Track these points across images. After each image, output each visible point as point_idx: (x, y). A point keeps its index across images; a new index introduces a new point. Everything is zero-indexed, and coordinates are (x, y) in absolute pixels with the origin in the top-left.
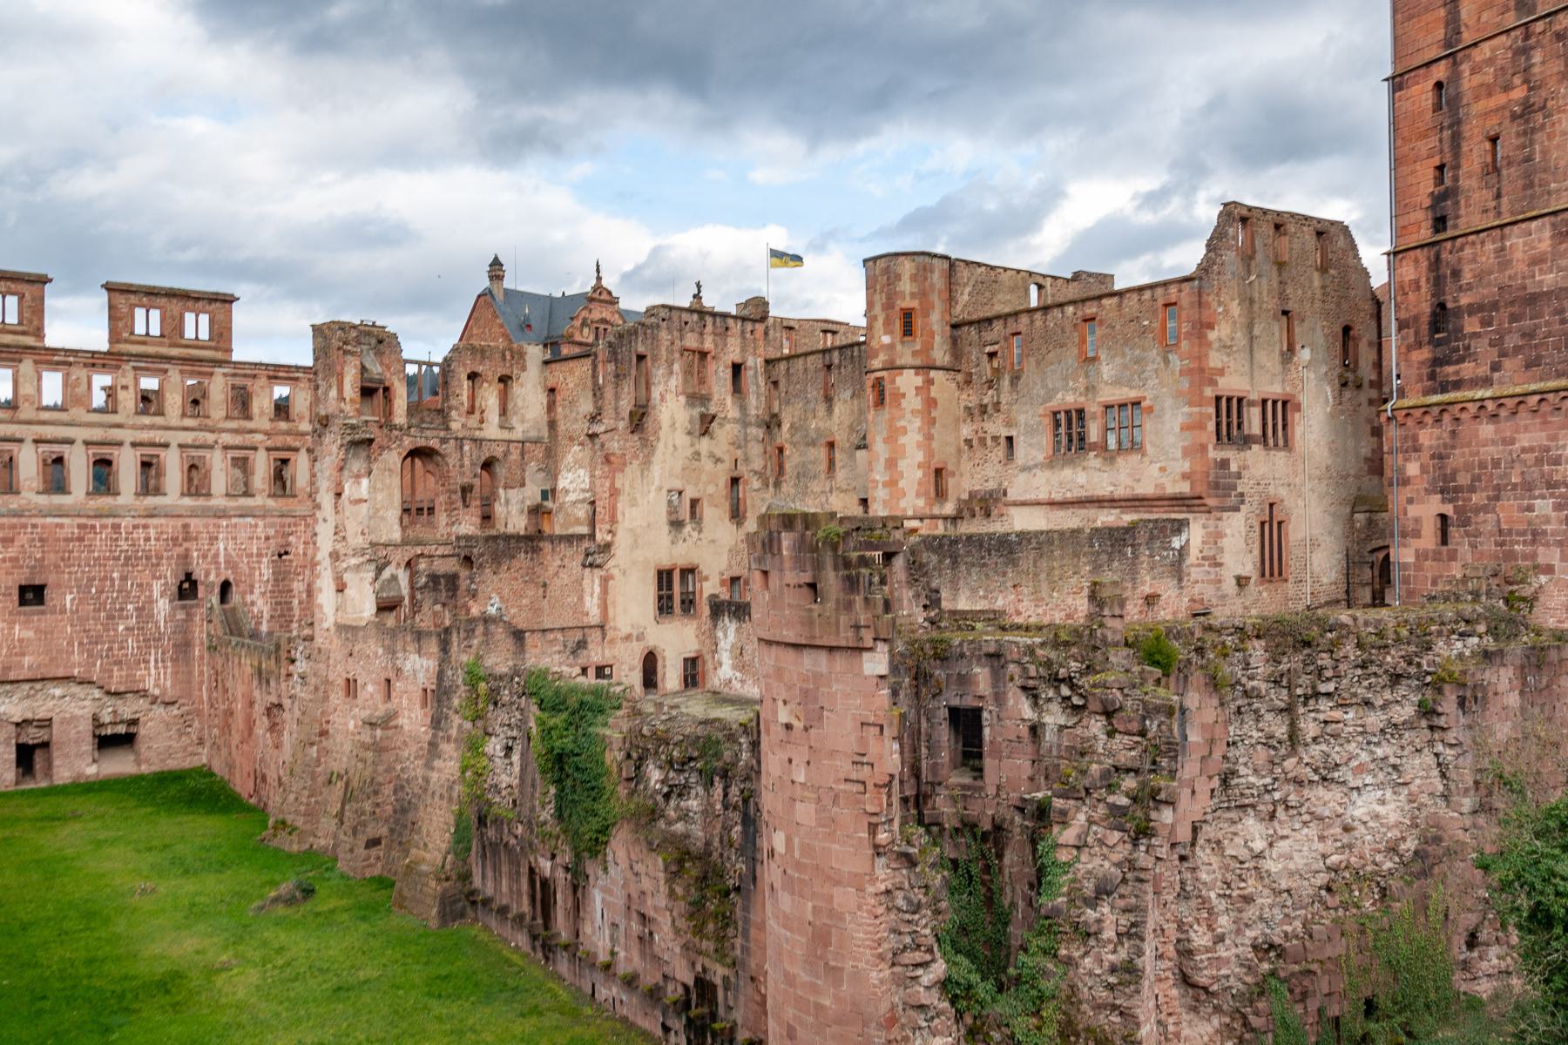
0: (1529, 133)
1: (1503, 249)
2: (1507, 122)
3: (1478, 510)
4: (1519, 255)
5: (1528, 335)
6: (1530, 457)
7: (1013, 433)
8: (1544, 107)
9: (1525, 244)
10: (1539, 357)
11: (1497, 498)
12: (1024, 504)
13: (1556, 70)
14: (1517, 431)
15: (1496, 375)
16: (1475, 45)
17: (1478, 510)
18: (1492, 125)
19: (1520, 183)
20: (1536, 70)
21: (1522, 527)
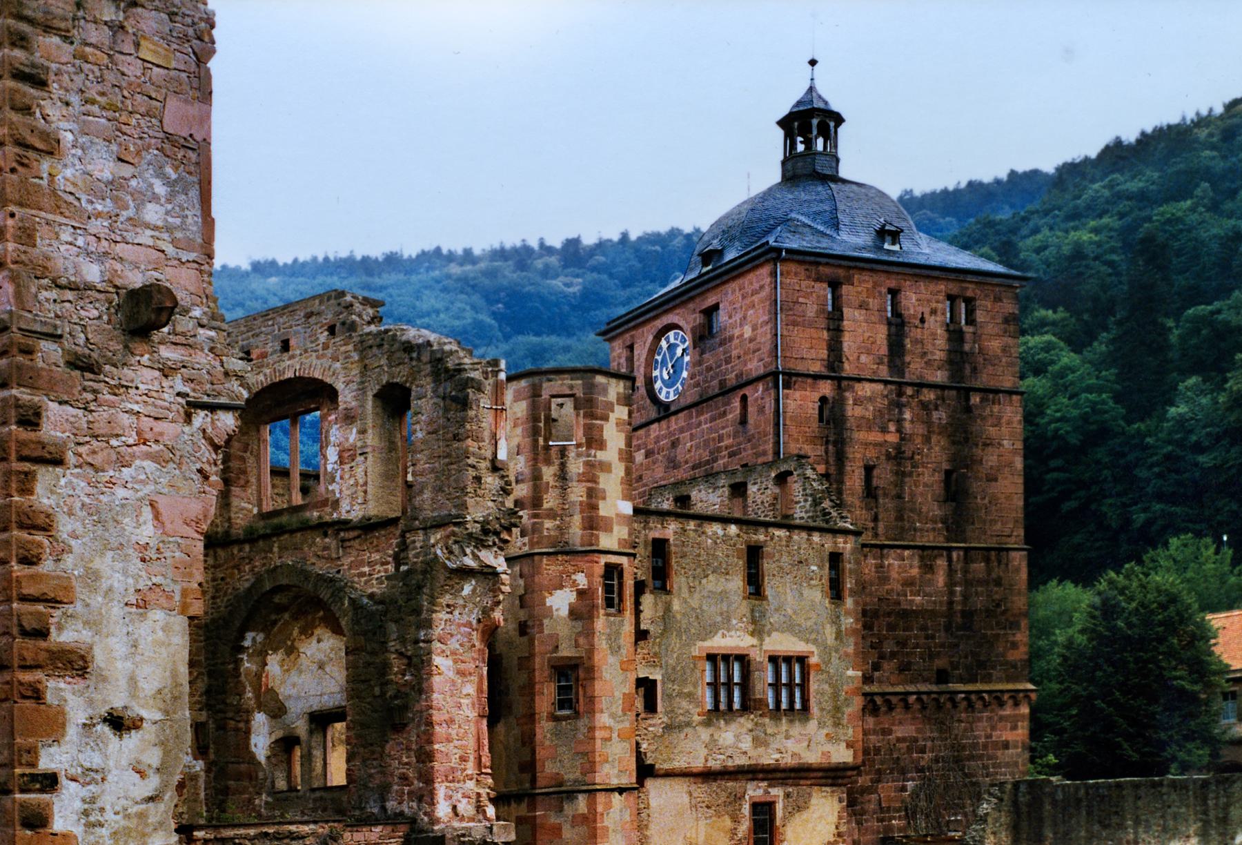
0: (901, 475)
1: (882, 566)
2: (883, 458)
3: (865, 790)
4: (894, 575)
5: (902, 643)
6: (904, 745)
7: (657, 675)
8: (912, 458)
9: (900, 567)
10: (909, 663)
11: (879, 781)
12: (669, 774)
13: (921, 431)
14: (893, 724)
15: (877, 674)
16: (859, 380)
17: (865, 790)
18: (871, 453)
19: (893, 515)
20: (907, 425)
21: (898, 805)
